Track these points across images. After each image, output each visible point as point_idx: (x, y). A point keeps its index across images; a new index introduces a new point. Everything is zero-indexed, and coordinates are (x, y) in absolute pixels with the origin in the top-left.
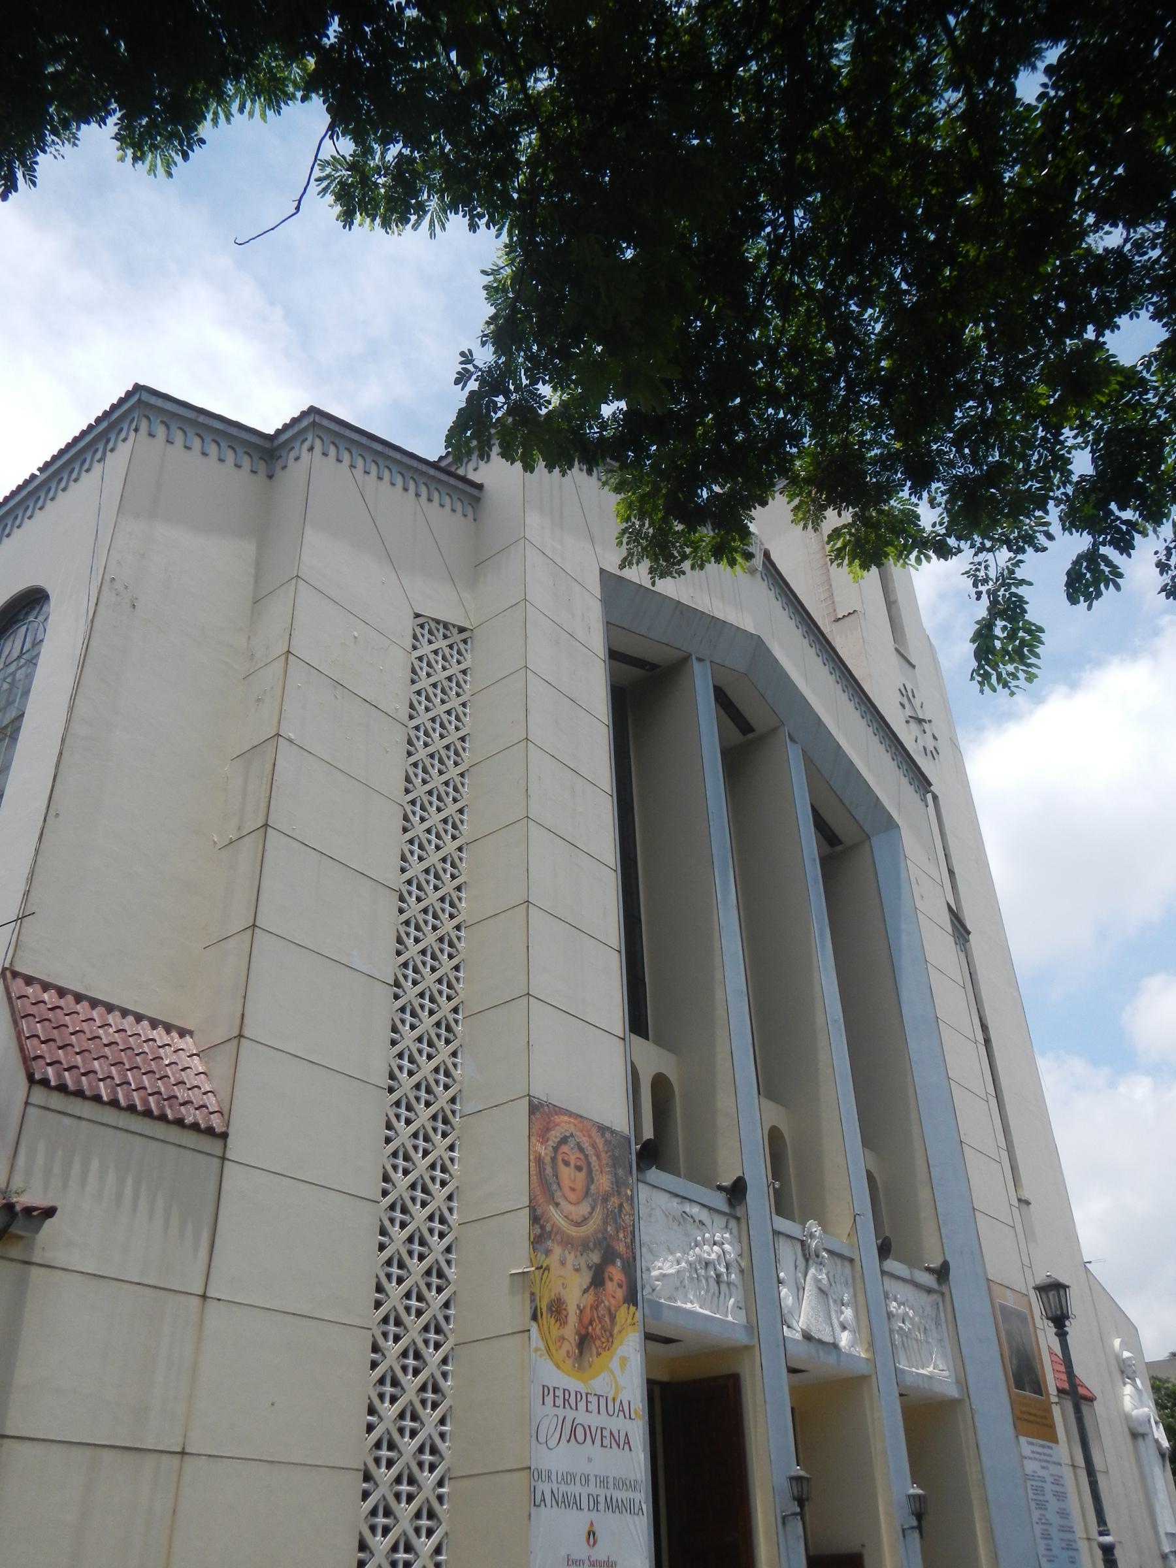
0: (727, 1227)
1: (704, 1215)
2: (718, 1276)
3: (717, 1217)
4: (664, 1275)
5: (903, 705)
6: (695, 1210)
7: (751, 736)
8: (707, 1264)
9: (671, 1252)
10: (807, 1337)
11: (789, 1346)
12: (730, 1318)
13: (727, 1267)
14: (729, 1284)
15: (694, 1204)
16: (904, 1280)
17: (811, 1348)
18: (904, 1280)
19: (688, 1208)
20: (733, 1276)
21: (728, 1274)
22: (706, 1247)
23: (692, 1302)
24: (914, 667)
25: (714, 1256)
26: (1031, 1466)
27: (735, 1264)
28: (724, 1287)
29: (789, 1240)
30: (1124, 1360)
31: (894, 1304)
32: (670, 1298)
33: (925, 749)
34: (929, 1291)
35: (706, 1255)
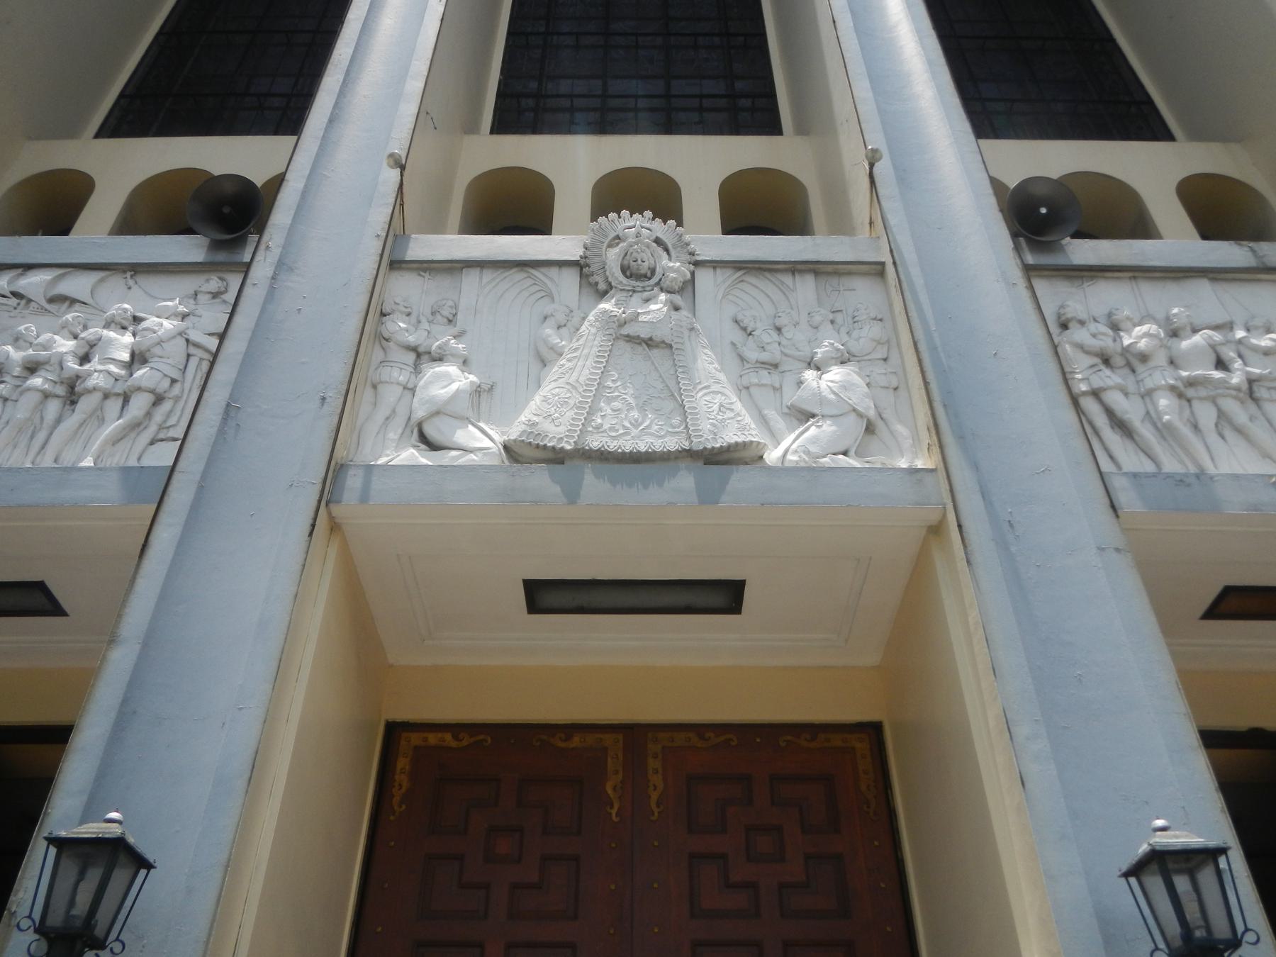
17: (540, 480)
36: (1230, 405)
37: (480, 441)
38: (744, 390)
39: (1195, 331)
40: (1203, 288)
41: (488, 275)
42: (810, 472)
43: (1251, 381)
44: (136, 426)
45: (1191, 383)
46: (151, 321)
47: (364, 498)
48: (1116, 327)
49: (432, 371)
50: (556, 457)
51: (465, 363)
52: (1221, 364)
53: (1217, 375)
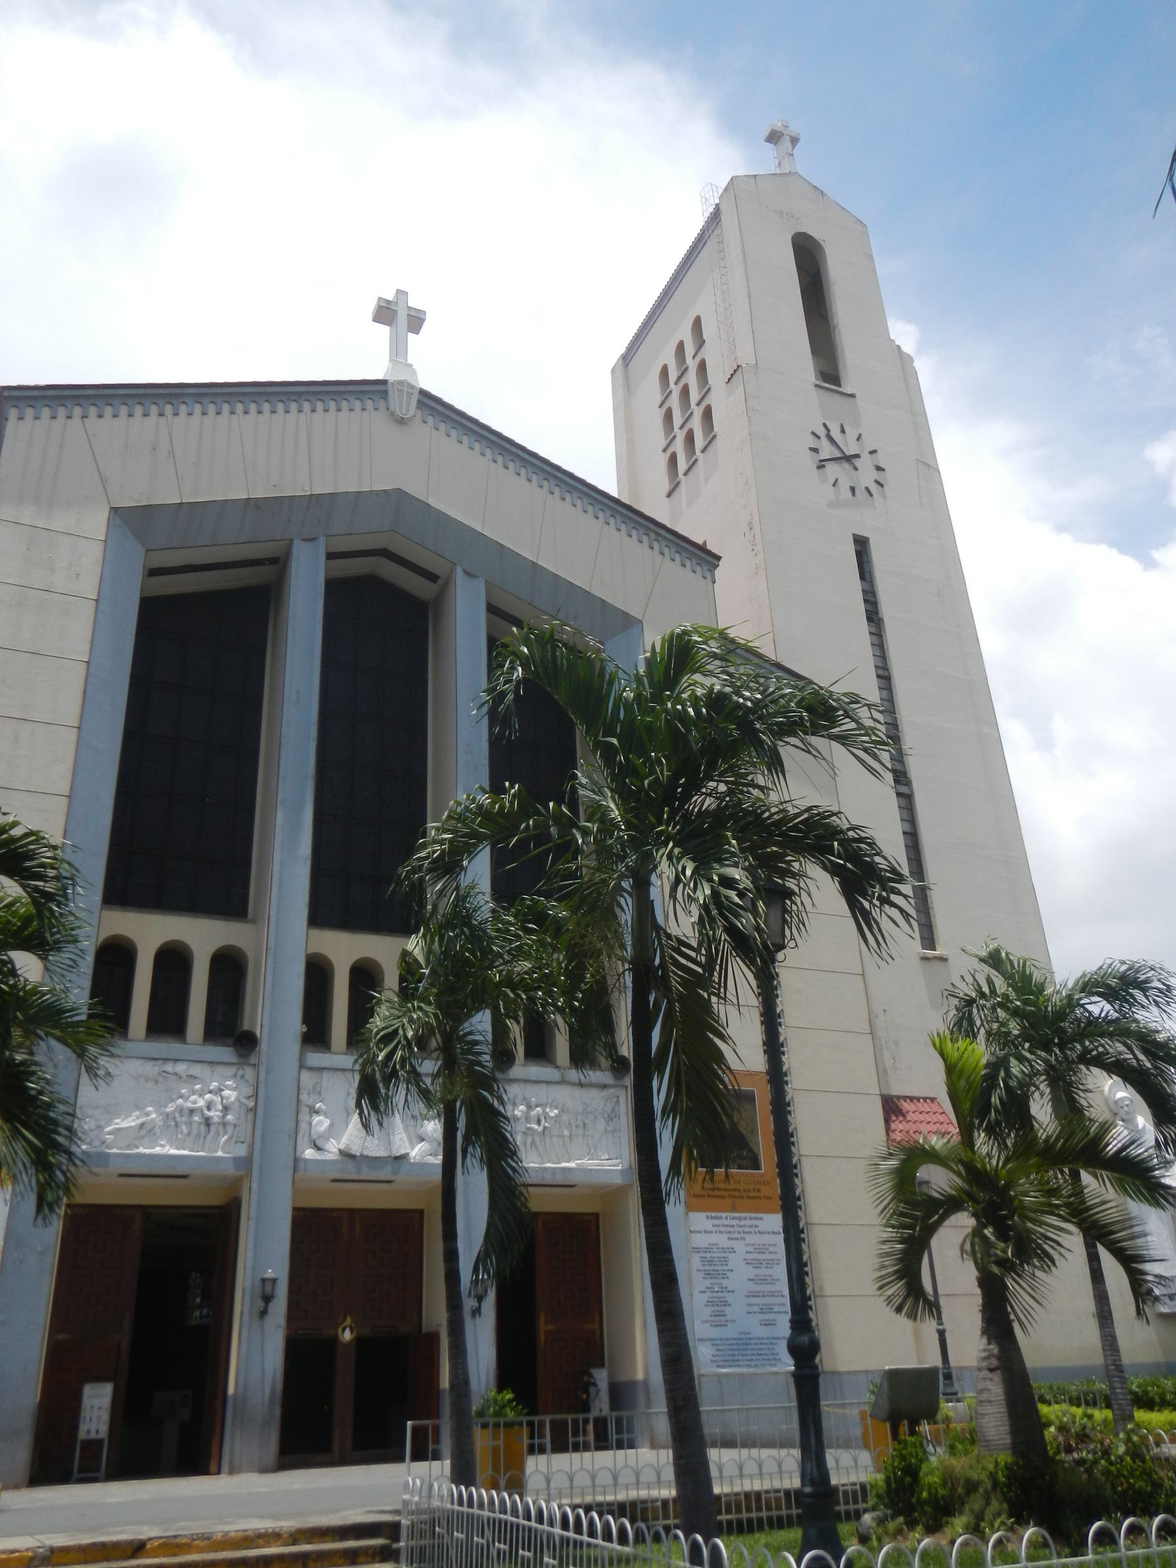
0: (235, 1075)
1: (196, 1070)
2: (208, 1122)
3: (220, 1070)
4: (120, 1129)
5: (815, 450)
6: (181, 1068)
7: (440, 582)
8: (192, 1111)
9: (138, 1107)
10: (346, 1155)
11: (301, 1165)
12: (220, 1153)
13: (226, 1109)
14: (224, 1124)
15: (179, 1063)
16: (548, 1083)
17: (350, 1165)
18: (548, 1083)
19: (169, 1067)
20: (229, 1117)
21: (224, 1116)
22: (193, 1098)
23: (163, 1146)
24: (852, 396)
25: (201, 1103)
26: (700, 1241)
27: (237, 1105)
28: (213, 1129)
29: (340, 1073)
30: (1116, 1102)
31: (522, 1108)
32: (129, 1147)
33: (853, 489)
34: (604, 1087)
35: (190, 1105)
36: (537, 1139)
37: (333, 1148)
38: (406, 1127)
39: (537, 1106)
40: (544, 1086)
41: (331, 1073)
42: (422, 1165)
43: (545, 1128)
44: (231, 1138)
45: (529, 1128)
46: (226, 1093)
47: (306, 1170)
48: (515, 1105)
49: (317, 1119)
50: (353, 1157)
51: (325, 1115)
52: (539, 1122)
53: (535, 1127)
